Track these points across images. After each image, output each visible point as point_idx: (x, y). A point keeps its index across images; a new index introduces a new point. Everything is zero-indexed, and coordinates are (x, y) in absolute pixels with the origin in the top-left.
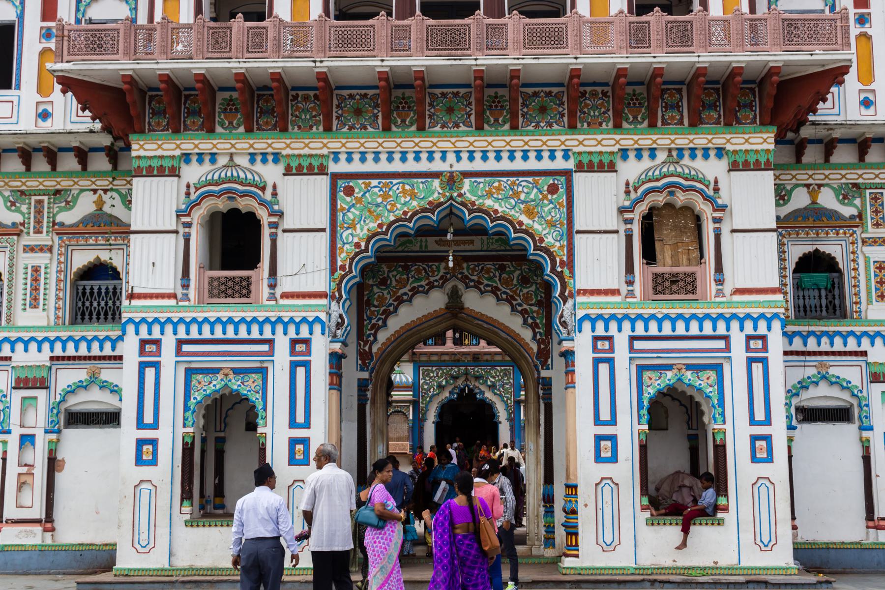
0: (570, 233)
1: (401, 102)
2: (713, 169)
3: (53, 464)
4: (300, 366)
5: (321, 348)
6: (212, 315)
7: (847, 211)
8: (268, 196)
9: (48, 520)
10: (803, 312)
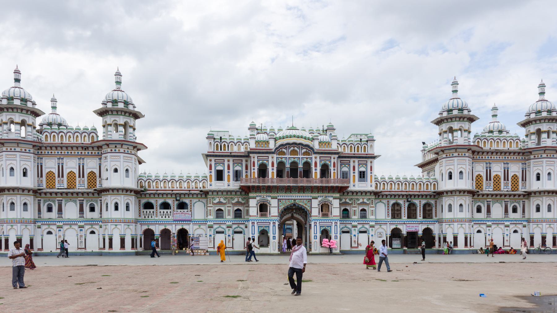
0: (311, 208)
1: (289, 189)
2: (331, 199)
3: (233, 239)
4: (274, 226)
5: (277, 224)
7: (350, 202)
10: (343, 217)
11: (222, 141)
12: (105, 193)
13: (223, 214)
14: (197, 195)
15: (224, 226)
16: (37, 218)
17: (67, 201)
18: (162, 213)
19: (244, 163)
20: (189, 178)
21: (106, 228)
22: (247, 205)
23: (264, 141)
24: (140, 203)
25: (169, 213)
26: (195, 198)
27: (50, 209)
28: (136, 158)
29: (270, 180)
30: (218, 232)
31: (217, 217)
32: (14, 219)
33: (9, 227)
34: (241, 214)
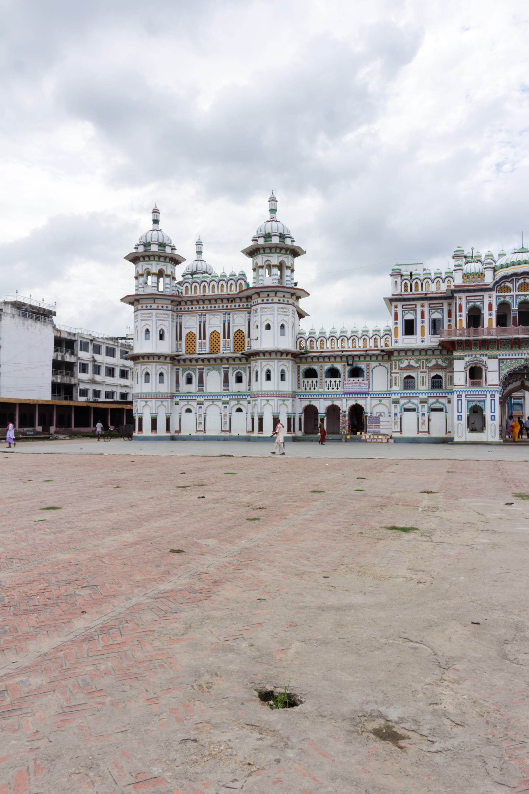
1: (516, 344)
3: (429, 420)
5: (497, 396)
6: (473, 389)
8: (484, 363)
9: (428, 432)
11: (413, 277)
12: (255, 358)
13: (414, 382)
14: (377, 356)
15: (416, 401)
16: (174, 391)
17: (209, 370)
18: (328, 383)
19: (446, 308)
20: (365, 333)
21: (255, 405)
22: (450, 369)
23: (476, 274)
24: (299, 370)
25: (338, 382)
26: (374, 361)
27: (189, 381)
28: (295, 309)
29: (486, 331)
30: (407, 410)
31: (406, 387)
32: (148, 393)
33: (143, 403)
34: (441, 382)
